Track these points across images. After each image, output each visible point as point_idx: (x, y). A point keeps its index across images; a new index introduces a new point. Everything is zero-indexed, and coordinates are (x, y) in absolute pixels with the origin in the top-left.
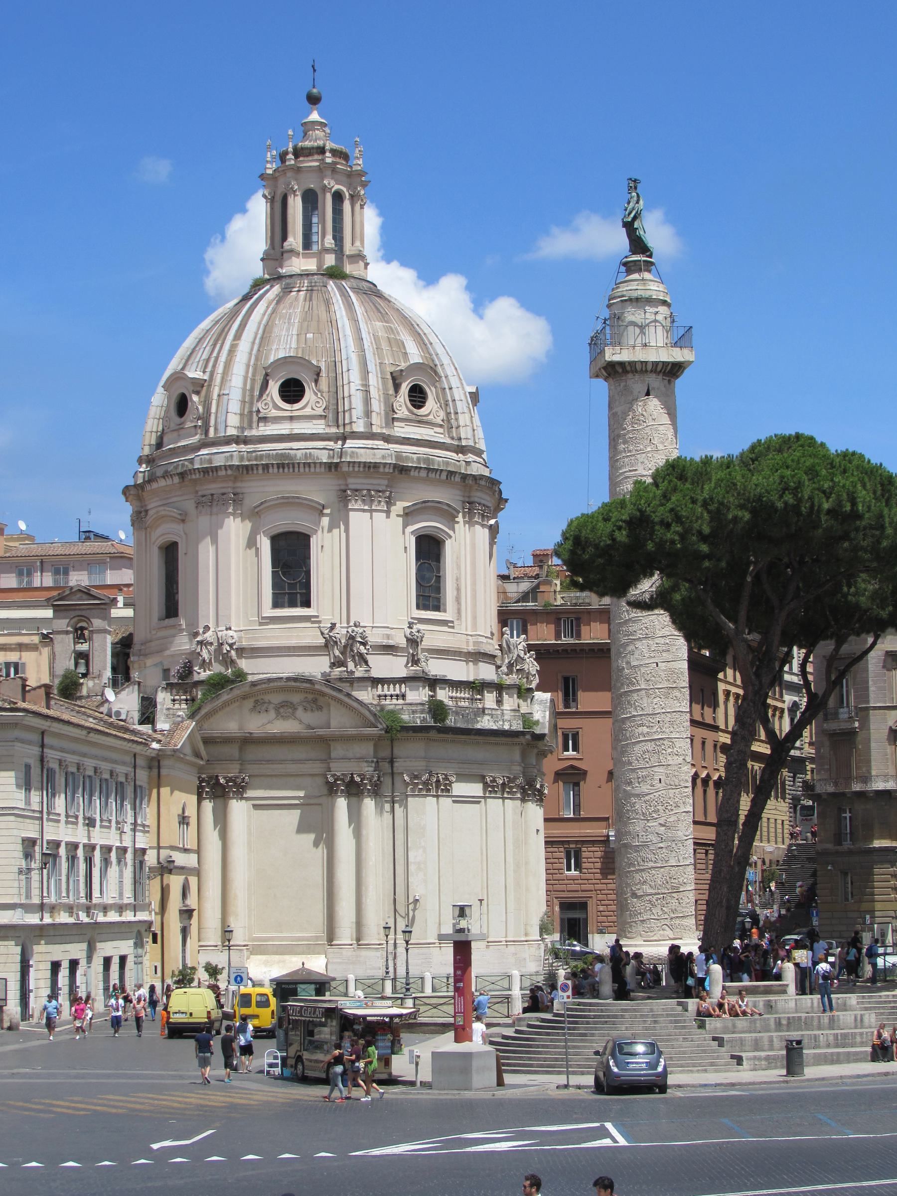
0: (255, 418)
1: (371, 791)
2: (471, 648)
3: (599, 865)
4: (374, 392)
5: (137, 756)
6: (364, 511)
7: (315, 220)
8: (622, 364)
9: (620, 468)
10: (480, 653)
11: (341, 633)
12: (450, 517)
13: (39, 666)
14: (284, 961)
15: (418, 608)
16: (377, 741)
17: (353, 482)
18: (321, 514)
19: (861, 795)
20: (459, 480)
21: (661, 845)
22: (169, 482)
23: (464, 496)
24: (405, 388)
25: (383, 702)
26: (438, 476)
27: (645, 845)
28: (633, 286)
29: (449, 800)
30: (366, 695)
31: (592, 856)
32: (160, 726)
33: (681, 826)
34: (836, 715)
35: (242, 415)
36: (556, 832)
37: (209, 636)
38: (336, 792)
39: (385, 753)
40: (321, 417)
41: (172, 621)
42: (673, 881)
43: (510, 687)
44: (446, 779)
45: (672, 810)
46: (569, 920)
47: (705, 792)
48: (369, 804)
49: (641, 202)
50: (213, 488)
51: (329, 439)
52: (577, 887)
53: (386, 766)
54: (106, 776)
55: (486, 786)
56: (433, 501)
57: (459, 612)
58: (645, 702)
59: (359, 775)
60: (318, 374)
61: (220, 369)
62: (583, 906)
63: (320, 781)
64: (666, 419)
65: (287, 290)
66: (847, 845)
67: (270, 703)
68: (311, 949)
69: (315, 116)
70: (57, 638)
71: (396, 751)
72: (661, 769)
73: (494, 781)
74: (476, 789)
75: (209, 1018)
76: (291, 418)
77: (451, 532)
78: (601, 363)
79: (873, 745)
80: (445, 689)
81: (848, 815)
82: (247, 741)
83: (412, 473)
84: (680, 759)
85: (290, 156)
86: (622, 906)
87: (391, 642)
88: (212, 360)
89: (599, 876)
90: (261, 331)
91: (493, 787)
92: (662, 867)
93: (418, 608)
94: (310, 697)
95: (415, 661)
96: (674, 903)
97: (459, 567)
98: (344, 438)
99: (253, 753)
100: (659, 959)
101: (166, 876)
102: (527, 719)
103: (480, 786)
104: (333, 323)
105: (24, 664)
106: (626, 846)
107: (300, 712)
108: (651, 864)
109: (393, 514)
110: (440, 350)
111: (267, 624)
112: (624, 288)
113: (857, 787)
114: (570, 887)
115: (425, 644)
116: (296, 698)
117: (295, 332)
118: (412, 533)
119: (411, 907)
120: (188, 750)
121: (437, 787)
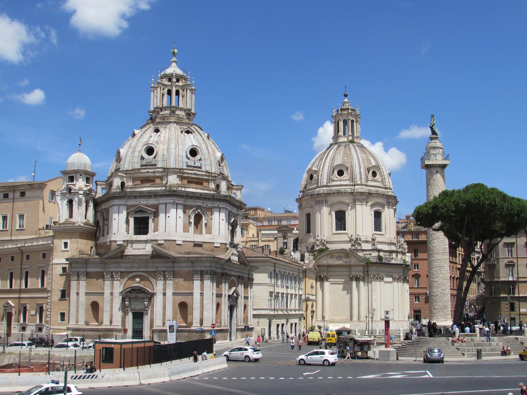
0: (331, 180)
2: (389, 241)
3: (424, 300)
4: (362, 173)
6: (360, 205)
7: (346, 128)
8: (430, 165)
9: (430, 193)
10: (391, 243)
11: (354, 237)
12: (383, 206)
13: (274, 246)
14: (339, 325)
15: (375, 231)
16: (364, 266)
17: (357, 197)
18: (349, 206)
19: (497, 282)
22: (308, 197)
24: (371, 172)
25: (365, 256)
27: (437, 295)
28: (433, 144)
29: (383, 282)
30: (361, 254)
31: (422, 298)
32: (305, 262)
33: (447, 290)
34: (490, 260)
35: (327, 179)
36: (412, 291)
37: (319, 238)
38: (353, 280)
39: (366, 269)
40: (348, 180)
41: (309, 234)
43: (400, 252)
44: (382, 276)
46: (416, 315)
47: (453, 281)
48: (362, 283)
49: (435, 121)
50: (320, 199)
51: (351, 186)
52: (418, 306)
53: (366, 273)
54: (291, 275)
55: (393, 278)
57: (386, 232)
58: (437, 256)
59: (359, 275)
60: (348, 169)
61: (321, 167)
62: (420, 311)
63: (348, 277)
64: (442, 180)
65: (339, 146)
66: (493, 295)
67: (335, 256)
68: (346, 322)
69: (346, 100)
70: (279, 238)
71: (369, 269)
73: (395, 277)
74: (390, 279)
75: (319, 340)
76: (340, 180)
77: (383, 211)
78: (424, 165)
79: (500, 268)
81: (493, 287)
82: (329, 266)
83: (373, 195)
84: (447, 272)
85: (340, 111)
86: (431, 312)
87: (367, 240)
88: (319, 165)
89: (424, 303)
90: (332, 157)
91: (395, 279)
94: (346, 254)
95: (374, 245)
96: (445, 311)
98: (355, 185)
99: (330, 269)
101: (307, 302)
102: (404, 261)
103: (392, 278)
104: (351, 154)
105: (270, 245)
106: (432, 295)
107: (343, 259)
108: (439, 300)
109: (368, 206)
110: (380, 162)
111: (334, 235)
112: (430, 144)
113: (496, 280)
114: (416, 306)
115: (377, 240)
116: (342, 255)
117: (341, 157)
119: (373, 311)
120: (313, 268)
121: (380, 279)
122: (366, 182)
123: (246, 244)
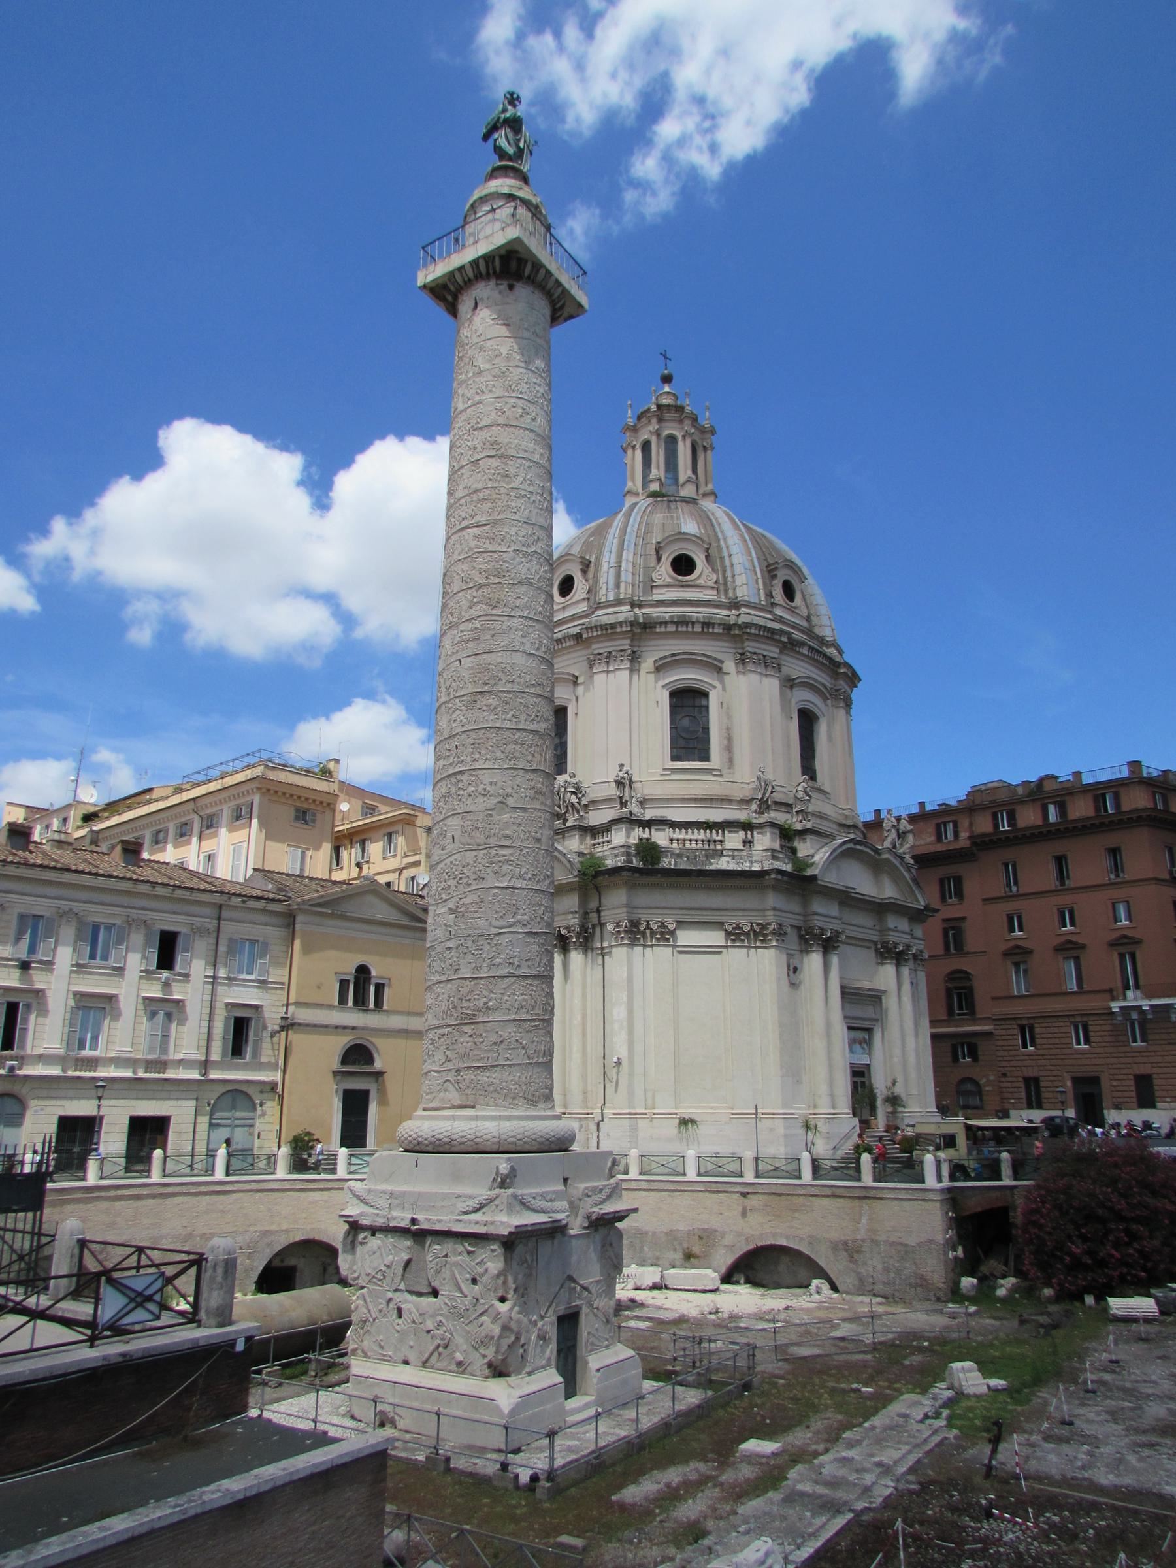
1: (578, 944)
5: (224, 908)
17: (597, 647)
20: (721, 631)
21: (449, 944)
23: (735, 648)
26: (690, 629)
42: (465, 1004)
43: (761, 826)
44: (663, 925)
45: (470, 884)
53: (594, 916)
55: (728, 934)
56: (684, 653)
57: (731, 761)
59: (566, 928)
62: (1094, 1081)
69: (667, 389)
71: (603, 901)
72: (454, 821)
73: (738, 927)
74: (715, 938)
77: (716, 683)
80: (664, 830)
83: (658, 630)
92: (448, 981)
93: (674, 758)
97: (729, 717)
100: (419, 1143)
103: (721, 934)
108: (437, 978)
109: (643, 672)
118: (663, 686)
121: (652, 937)
122: (645, 593)
123: (400, 874)
